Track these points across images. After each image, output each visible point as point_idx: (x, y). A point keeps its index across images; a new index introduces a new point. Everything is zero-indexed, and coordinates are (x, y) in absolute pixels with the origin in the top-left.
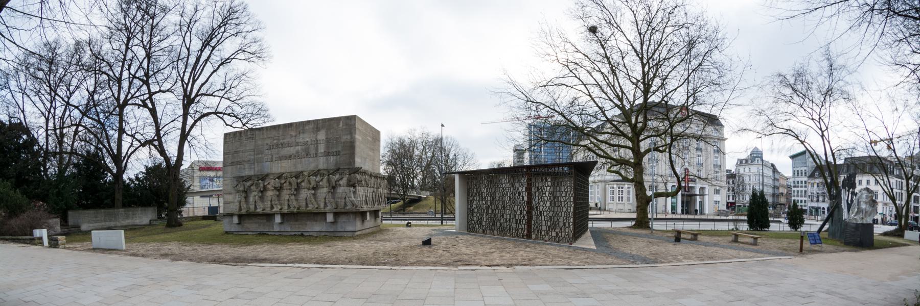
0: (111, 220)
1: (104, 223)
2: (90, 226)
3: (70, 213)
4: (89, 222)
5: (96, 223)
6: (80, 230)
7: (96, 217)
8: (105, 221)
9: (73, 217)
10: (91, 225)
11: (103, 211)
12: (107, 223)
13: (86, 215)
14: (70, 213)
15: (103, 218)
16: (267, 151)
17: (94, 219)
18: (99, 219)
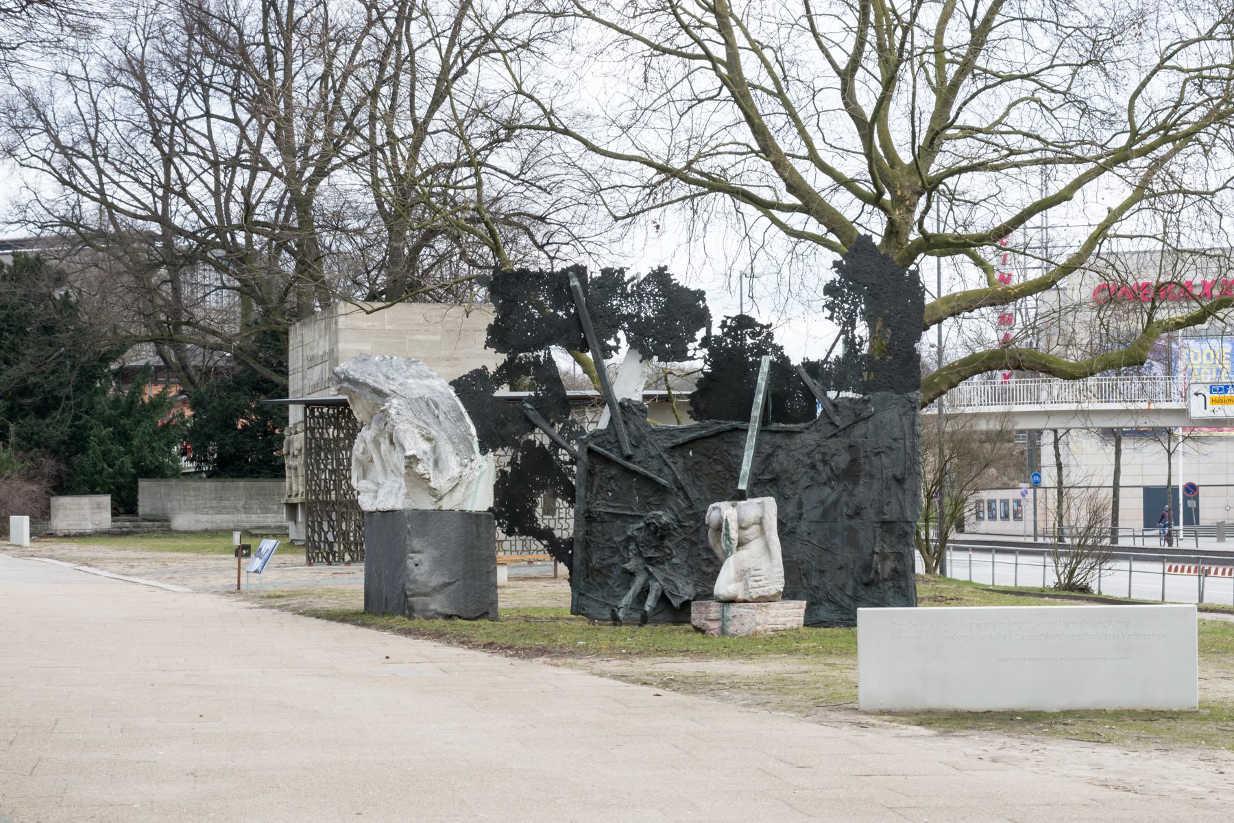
0: (266, 511)
1: (244, 517)
2: (198, 521)
3: (143, 484)
4: (196, 510)
5: (220, 513)
6: (168, 527)
7: (220, 499)
8: (248, 510)
9: (149, 495)
10: (204, 518)
11: (241, 484)
12: (254, 517)
13: (192, 493)
14: (143, 484)
15: (241, 504)
16: (309, 372)
17: (215, 503)
18: (228, 503)
